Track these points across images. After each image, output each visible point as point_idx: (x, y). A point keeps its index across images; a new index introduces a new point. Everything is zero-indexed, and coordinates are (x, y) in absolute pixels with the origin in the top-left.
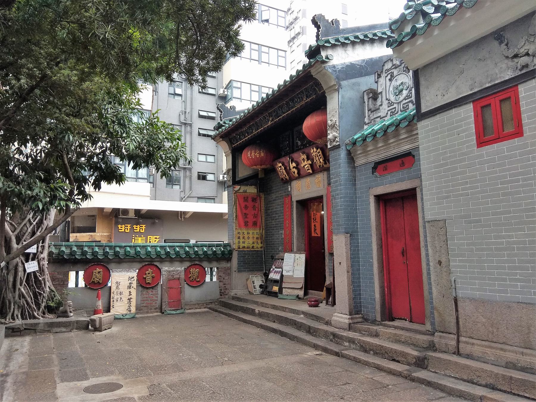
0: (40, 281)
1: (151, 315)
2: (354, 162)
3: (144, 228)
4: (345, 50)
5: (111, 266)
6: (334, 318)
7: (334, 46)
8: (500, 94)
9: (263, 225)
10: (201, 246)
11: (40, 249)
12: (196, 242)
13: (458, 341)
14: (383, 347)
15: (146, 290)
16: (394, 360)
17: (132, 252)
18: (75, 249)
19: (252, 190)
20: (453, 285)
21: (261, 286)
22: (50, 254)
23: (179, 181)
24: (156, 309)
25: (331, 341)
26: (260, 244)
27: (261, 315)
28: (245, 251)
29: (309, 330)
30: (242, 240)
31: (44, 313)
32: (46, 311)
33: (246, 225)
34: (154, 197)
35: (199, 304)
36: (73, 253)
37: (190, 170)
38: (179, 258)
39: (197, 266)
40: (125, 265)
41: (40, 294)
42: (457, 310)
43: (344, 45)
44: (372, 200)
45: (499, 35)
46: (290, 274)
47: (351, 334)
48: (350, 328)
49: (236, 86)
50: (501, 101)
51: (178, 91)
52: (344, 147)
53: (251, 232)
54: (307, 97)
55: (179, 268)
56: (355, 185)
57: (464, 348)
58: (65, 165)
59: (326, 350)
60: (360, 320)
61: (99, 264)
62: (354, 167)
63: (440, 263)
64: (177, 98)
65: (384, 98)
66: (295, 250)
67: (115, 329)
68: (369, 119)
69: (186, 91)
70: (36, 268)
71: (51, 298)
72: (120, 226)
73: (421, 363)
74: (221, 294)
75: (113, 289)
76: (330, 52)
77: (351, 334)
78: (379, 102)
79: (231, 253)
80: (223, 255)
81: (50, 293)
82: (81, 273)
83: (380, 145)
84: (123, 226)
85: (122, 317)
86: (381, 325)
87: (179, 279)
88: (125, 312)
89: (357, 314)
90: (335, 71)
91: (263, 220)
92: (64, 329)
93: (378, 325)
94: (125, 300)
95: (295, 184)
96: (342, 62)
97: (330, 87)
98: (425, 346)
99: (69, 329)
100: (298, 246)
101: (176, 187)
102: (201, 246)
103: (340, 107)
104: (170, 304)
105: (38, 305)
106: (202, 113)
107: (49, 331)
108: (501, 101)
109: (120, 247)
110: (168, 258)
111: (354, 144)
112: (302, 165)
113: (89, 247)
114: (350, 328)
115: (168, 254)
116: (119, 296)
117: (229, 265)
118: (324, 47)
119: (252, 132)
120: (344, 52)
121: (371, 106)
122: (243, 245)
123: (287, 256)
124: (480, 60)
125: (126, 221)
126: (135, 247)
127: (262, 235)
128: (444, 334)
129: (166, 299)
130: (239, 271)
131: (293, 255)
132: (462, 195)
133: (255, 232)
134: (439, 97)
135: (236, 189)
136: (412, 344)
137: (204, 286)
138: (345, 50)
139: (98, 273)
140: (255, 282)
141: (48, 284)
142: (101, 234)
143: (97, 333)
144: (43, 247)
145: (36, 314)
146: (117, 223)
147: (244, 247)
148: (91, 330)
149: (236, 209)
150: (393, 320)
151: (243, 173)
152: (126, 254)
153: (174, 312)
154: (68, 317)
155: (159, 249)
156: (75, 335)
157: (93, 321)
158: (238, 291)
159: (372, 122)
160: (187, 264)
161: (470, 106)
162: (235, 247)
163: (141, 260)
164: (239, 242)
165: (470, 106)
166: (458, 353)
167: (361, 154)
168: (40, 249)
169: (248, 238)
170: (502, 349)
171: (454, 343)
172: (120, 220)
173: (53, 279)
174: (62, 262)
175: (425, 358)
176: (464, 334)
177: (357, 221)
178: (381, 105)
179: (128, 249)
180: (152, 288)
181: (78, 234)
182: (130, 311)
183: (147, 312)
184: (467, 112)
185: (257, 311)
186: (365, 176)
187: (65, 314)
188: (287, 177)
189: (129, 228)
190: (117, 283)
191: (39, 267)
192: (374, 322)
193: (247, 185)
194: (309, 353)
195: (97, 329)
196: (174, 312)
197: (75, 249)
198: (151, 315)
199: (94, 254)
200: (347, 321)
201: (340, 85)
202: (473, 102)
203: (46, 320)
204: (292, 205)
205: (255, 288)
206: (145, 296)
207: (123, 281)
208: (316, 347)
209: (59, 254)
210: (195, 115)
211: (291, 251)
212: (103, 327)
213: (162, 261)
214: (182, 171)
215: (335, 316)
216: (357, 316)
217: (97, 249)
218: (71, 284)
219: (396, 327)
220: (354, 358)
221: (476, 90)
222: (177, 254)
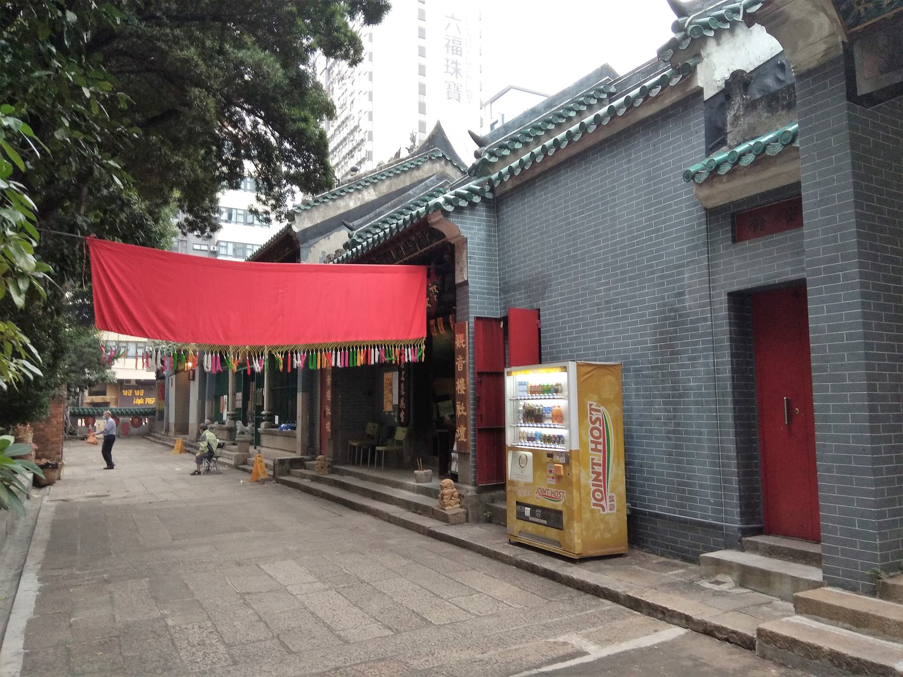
61: (90, 417)
74: (150, 430)
110: (122, 414)
125: (128, 388)
139: (90, 420)
146: (122, 389)
174: (75, 416)
218: (79, 424)
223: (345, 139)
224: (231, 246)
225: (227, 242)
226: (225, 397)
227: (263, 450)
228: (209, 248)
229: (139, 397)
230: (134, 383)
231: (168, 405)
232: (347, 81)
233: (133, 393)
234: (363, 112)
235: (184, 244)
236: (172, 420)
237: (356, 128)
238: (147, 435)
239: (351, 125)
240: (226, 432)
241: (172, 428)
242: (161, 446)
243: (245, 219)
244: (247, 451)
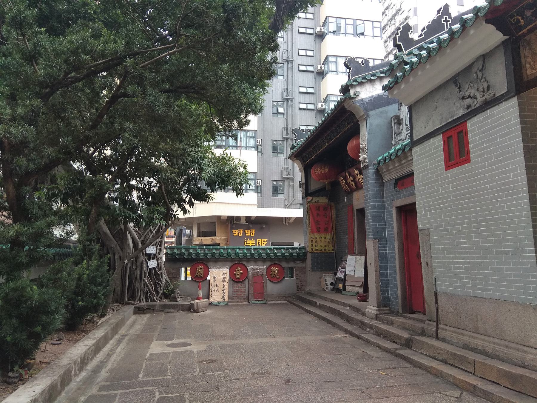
0: (158, 274)
1: (241, 303)
2: (382, 179)
3: (254, 232)
4: (373, 85)
5: (210, 264)
6: (367, 310)
7: (361, 84)
8: (457, 127)
9: (334, 231)
10: (280, 249)
11: (158, 251)
12: (300, 245)
13: (437, 328)
14: (388, 331)
15: (236, 284)
16: (394, 342)
17: (225, 253)
18: (183, 250)
19: (323, 200)
20: (434, 282)
21: (332, 284)
22: (167, 254)
23: (283, 190)
24: (244, 299)
25: (360, 327)
26: (331, 247)
27: (321, 307)
28: (318, 253)
29: (349, 320)
30: (314, 244)
31: (161, 299)
32: (163, 297)
33: (318, 231)
34: (262, 204)
35: (280, 297)
36: (182, 254)
37: (292, 179)
39: (276, 266)
40: (220, 263)
41: (159, 284)
42: (437, 302)
43: (371, 81)
44: (394, 211)
45: (455, 81)
46: (352, 273)
47: (377, 324)
48: (377, 317)
49: (333, 99)
50: (458, 133)
51: (281, 110)
52: (372, 167)
53: (323, 237)
54: (348, 124)
56: (383, 198)
57: (441, 334)
58: (163, 193)
59: (352, 334)
60: (388, 312)
62: (383, 183)
63: (427, 264)
64: (279, 116)
65: (404, 124)
66: (357, 253)
67: (208, 312)
68: (395, 141)
69: (287, 109)
70: (156, 265)
71: (167, 287)
72: (234, 231)
73: (408, 344)
74: (298, 289)
75: (212, 281)
76: (358, 89)
77: (377, 324)
78: (401, 127)
79: (305, 254)
80: (298, 256)
81: (166, 283)
82: (189, 269)
83: (397, 165)
84: (237, 231)
85: (217, 304)
86: (402, 316)
87: (262, 276)
88: (220, 300)
89: (385, 307)
90: (364, 104)
91: (334, 226)
92: (173, 310)
93: (400, 316)
94: (221, 292)
95: (355, 195)
96: (370, 95)
97: (361, 117)
98: (419, 332)
99: (176, 311)
100: (358, 250)
101: (281, 196)
102: (280, 249)
103: (369, 133)
104: (255, 296)
105: (157, 292)
107: (163, 311)
108: (458, 133)
109: (216, 249)
111: (379, 164)
112: (357, 179)
113: (209, 250)
114: (377, 317)
115: (252, 255)
116: (216, 288)
117: (304, 265)
118: (352, 86)
119: (316, 152)
120: (371, 87)
121: (396, 131)
122: (316, 248)
123: (349, 257)
124: (445, 99)
125: (239, 227)
126: (227, 249)
127: (333, 240)
128: (431, 323)
129: (252, 292)
130: (313, 270)
131: (354, 257)
132: (437, 209)
133: (327, 237)
134: (423, 128)
135: (309, 200)
136: (412, 331)
138: (373, 85)
139: (200, 269)
140: (327, 280)
141: (164, 277)
142: (219, 238)
143: (196, 314)
144: (160, 249)
145: (155, 298)
146: (232, 228)
147: (317, 250)
148: (191, 312)
149: (309, 217)
150: (413, 312)
151: (314, 186)
152: (221, 255)
153: (258, 303)
154: (177, 301)
155: (245, 251)
156: (180, 315)
157: (192, 304)
158: (312, 288)
159: (397, 143)
160: (269, 264)
161: (440, 137)
162: (309, 249)
163: (232, 260)
164: (312, 246)
165: (440, 137)
166: (437, 337)
167: (385, 172)
168: (158, 251)
169: (321, 242)
170: (462, 334)
171: (434, 329)
172: (234, 226)
173: (169, 274)
175: (411, 340)
176: (442, 322)
177: (385, 228)
178: (402, 129)
179: (222, 251)
180: (241, 282)
181: (203, 238)
182: (224, 300)
183: (238, 302)
184: (438, 141)
185: (318, 304)
186: (389, 190)
187: (174, 299)
188: (349, 189)
189: (241, 232)
190: (214, 277)
191: (158, 264)
192: (397, 314)
193: (318, 196)
194: (338, 336)
195: (196, 311)
196: (258, 303)
197: (183, 250)
198: (241, 303)
199: (197, 254)
200: (375, 312)
201: (368, 116)
202: (443, 133)
203: (161, 303)
204: (353, 213)
205: (327, 285)
206: (236, 288)
207: (219, 275)
208: (346, 331)
209: (172, 254)
211: (353, 253)
212: (200, 310)
213: (248, 261)
214: (286, 181)
215: (369, 308)
216: (385, 308)
217: (199, 251)
219: (414, 319)
220: (367, 339)
221: (443, 124)
222: (260, 255)
224: (342, 61)
229: (250, 237)
230: (243, 221)
233: (244, 233)
238: (299, 300)
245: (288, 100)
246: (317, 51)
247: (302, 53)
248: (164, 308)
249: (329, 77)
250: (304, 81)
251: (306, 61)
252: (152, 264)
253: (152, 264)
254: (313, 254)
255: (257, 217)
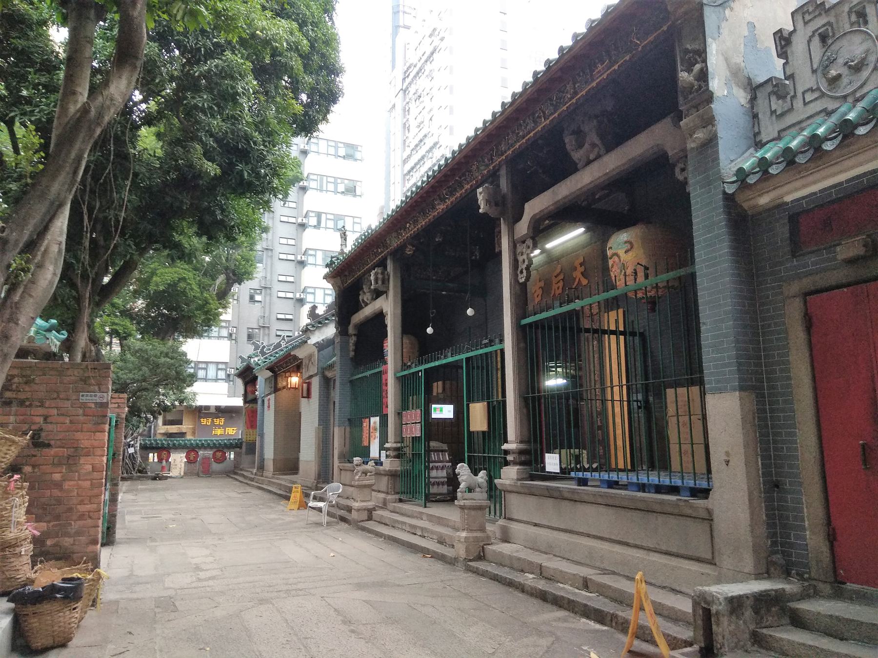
5: (171, 451)
36: (151, 444)
38: (207, 447)
55: (209, 453)
61: (163, 450)
64: (256, 304)
79: (241, 443)
82: (156, 455)
106: (280, 316)
110: (203, 447)
114: (256, 474)
125: (207, 415)
137: (225, 463)
146: (200, 417)
163: (188, 448)
174: (146, 448)
181: (169, 427)
187: (146, 473)
199: (163, 444)
207: (178, 459)
210: (273, 318)
213: (200, 448)
218: (151, 460)
222: (209, 444)
223: (423, 158)
224: (320, 255)
225: (316, 250)
226: (375, 420)
227: (514, 527)
228: (296, 258)
229: (219, 426)
230: (213, 410)
231: (262, 436)
232: (426, 99)
234: (443, 127)
235: (270, 253)
236: (269, 453)
237: (436, 144)
238: (233, 472)
239: (429, 142)
240: (385, 480)
241: (269, 465)
242: (259, 492)
243: (336, 224)
244: (482, 529)
245: (265, 288)
246: (298, 239)
247: (283, 241)
248: (139, 478)
249: (307, 270)
250: (284, 269)
251: (286, 249)
252: (131, 450)
253: (131, 450)
254: (247, 443)
255: (226, 407)
